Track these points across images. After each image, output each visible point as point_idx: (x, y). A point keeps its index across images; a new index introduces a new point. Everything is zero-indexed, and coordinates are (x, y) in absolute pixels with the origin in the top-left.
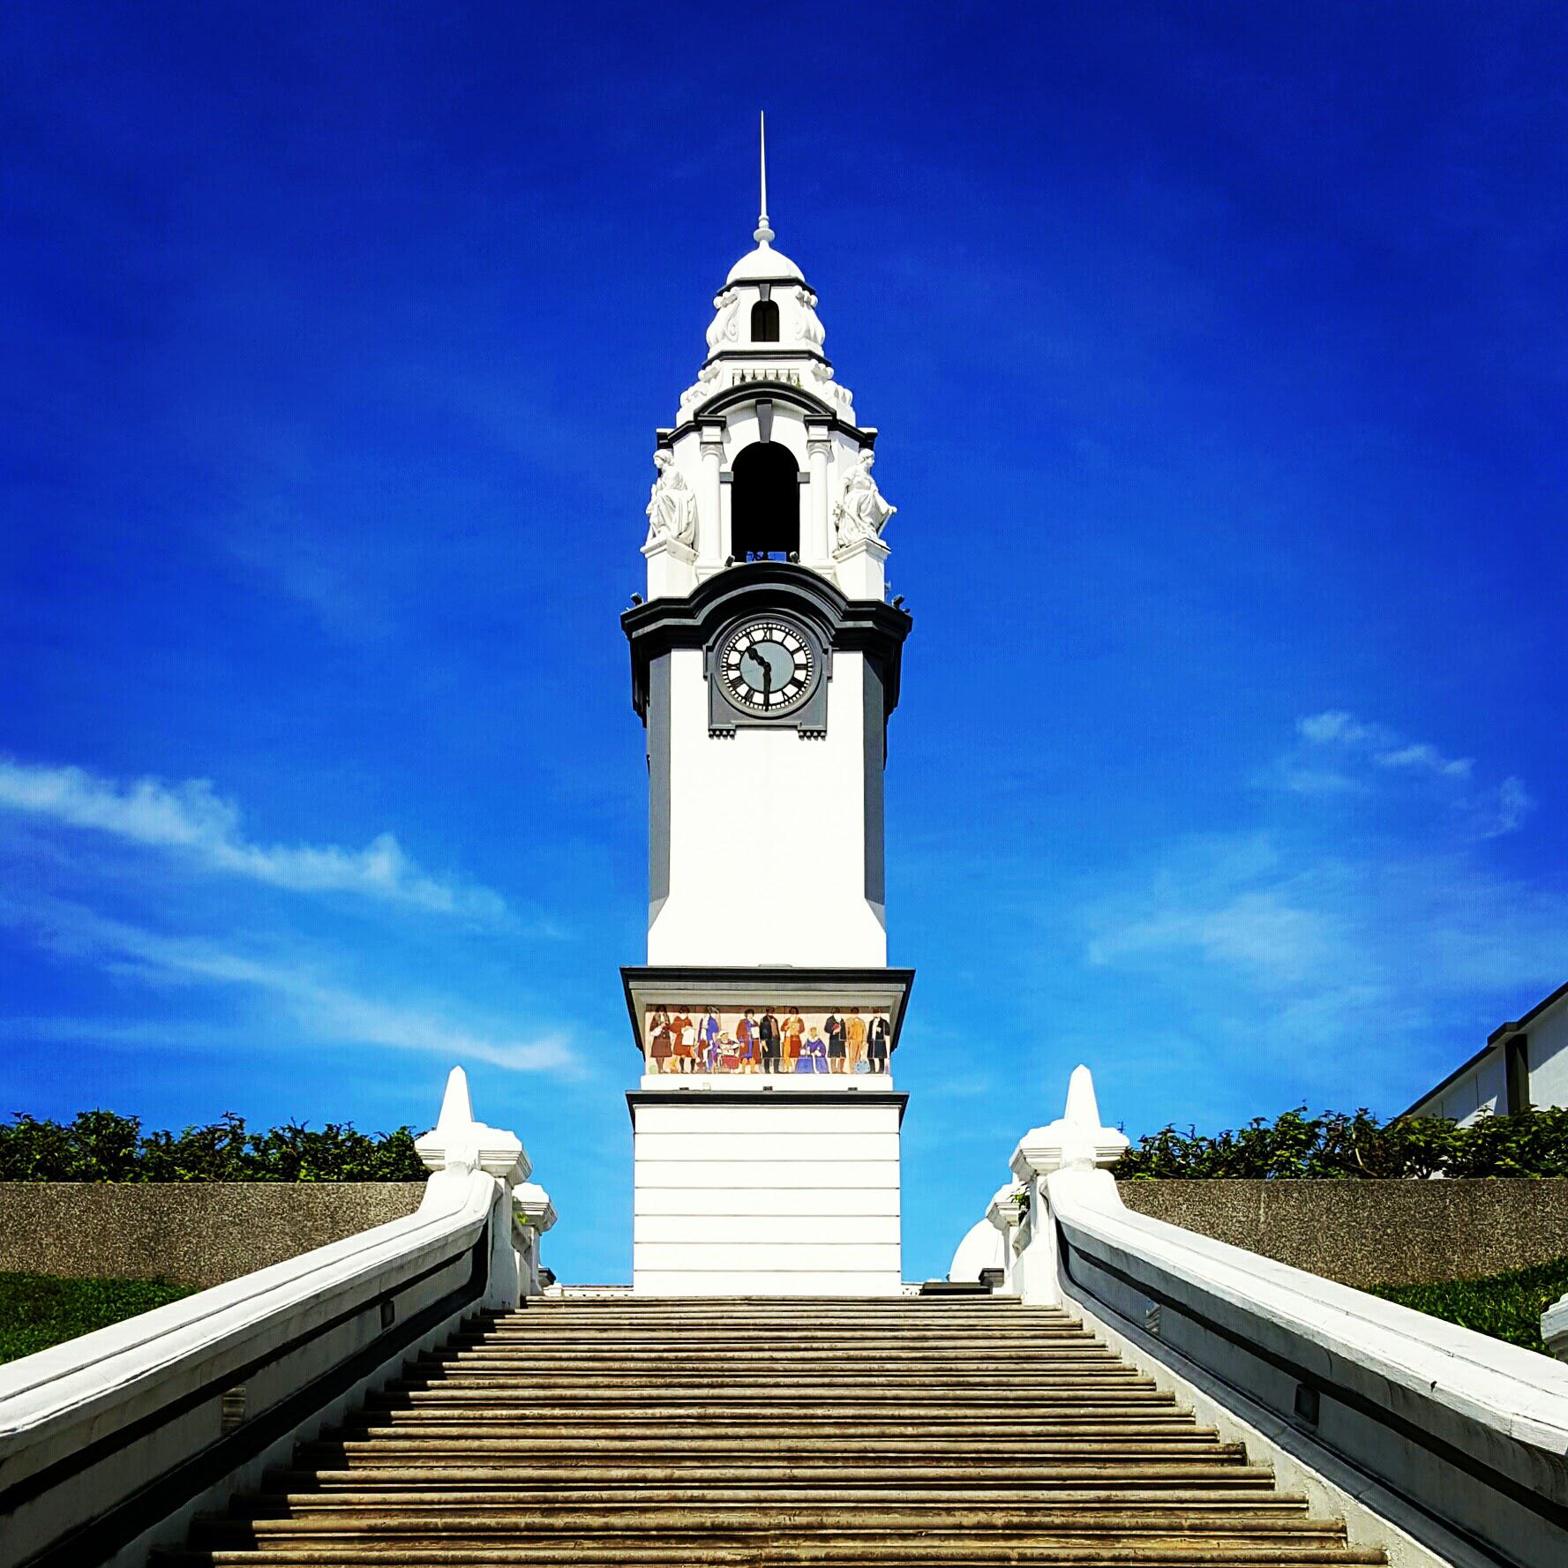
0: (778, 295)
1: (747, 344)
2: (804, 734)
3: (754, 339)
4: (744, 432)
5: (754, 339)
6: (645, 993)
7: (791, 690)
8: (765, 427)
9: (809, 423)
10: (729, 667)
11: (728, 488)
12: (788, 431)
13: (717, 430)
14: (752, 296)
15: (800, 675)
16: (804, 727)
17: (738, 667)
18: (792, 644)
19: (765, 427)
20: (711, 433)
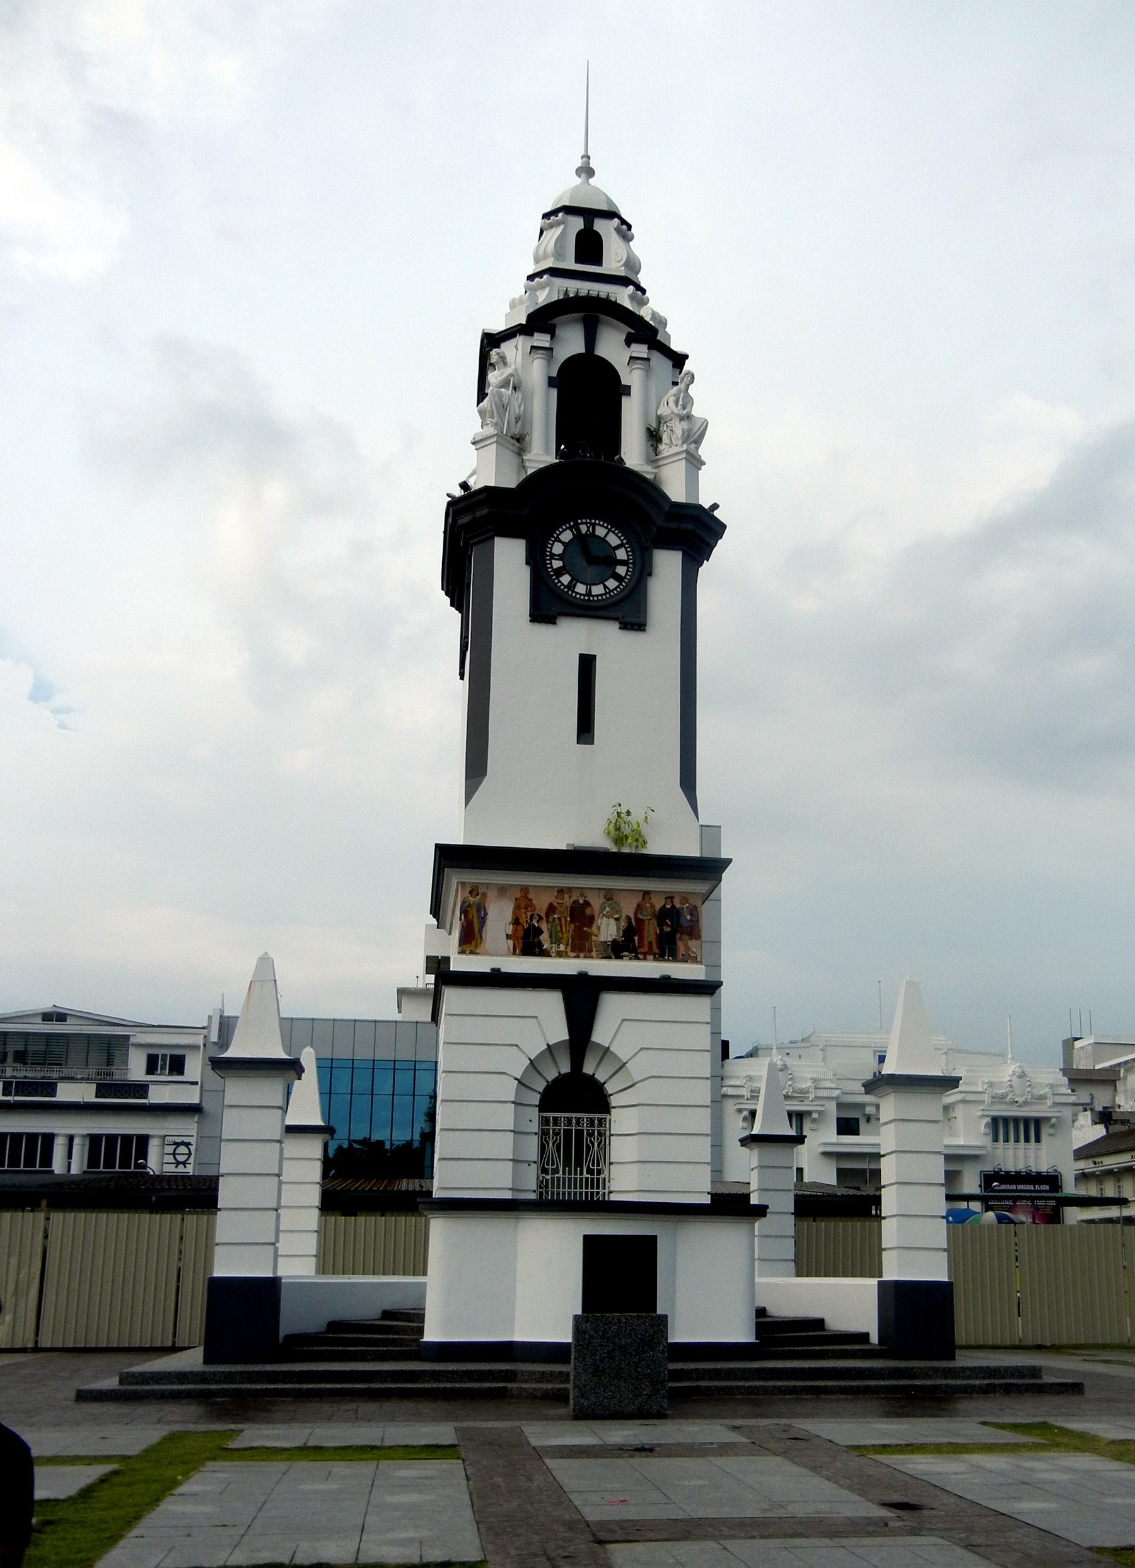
0: (600, 225)
1: (570, 264)
2: (626, 626)
3: (578, 260)
4: (571, 342)
5: (578, 260)
6: (455, 879)
7: (612, 584)
8: (591, 340)
9: (629, 342)
10: (553, 556)
11: (554, 392)
12: (613, 347)
13: (547, 337)
14: (578, 223)
15: (621, 570)
16: (628, 620)
17: (561, 557)
18: (613, 540)
19: (591, 340)
20: (541, 339)
